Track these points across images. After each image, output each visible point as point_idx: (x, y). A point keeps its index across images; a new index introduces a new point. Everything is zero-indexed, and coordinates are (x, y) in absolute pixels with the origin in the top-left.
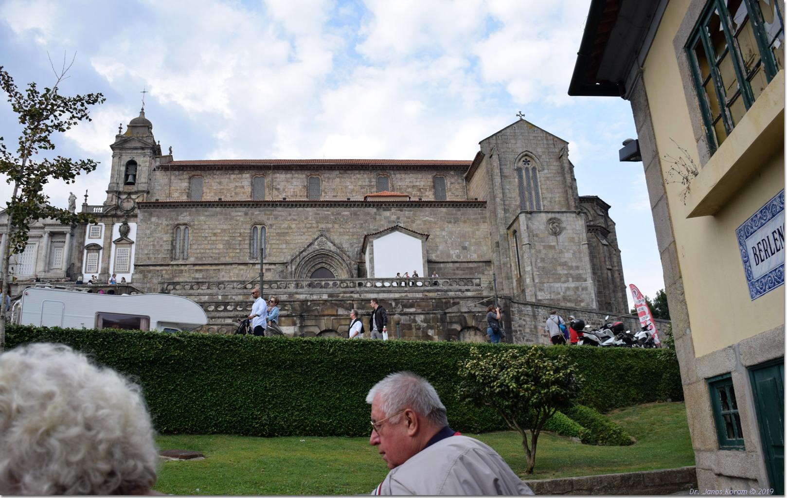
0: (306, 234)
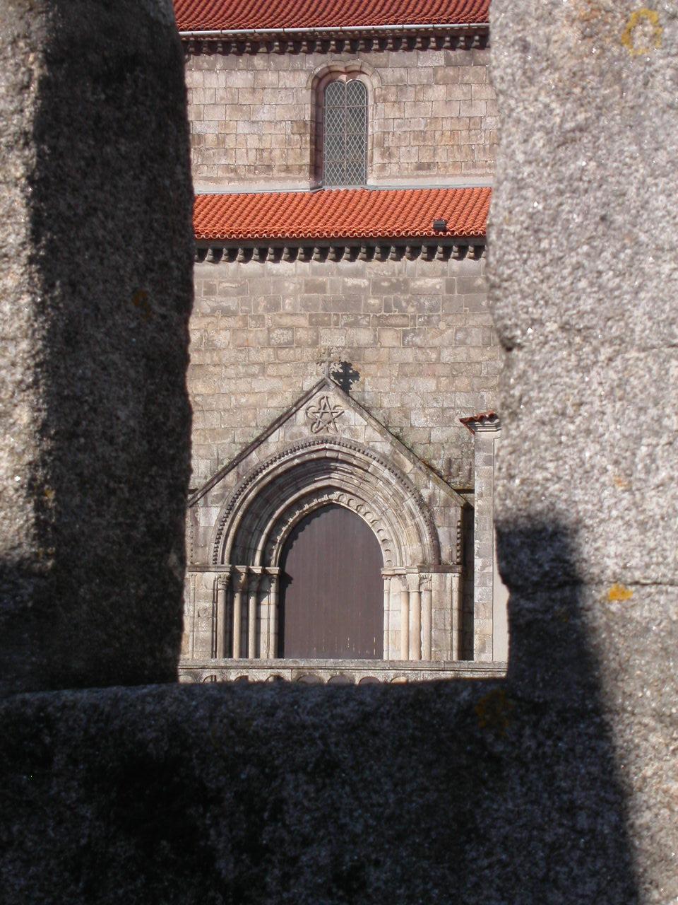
0: (271, 370)
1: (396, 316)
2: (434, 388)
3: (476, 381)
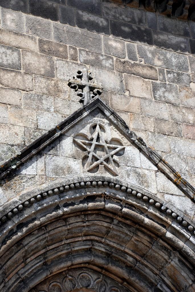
1: (143, 67)
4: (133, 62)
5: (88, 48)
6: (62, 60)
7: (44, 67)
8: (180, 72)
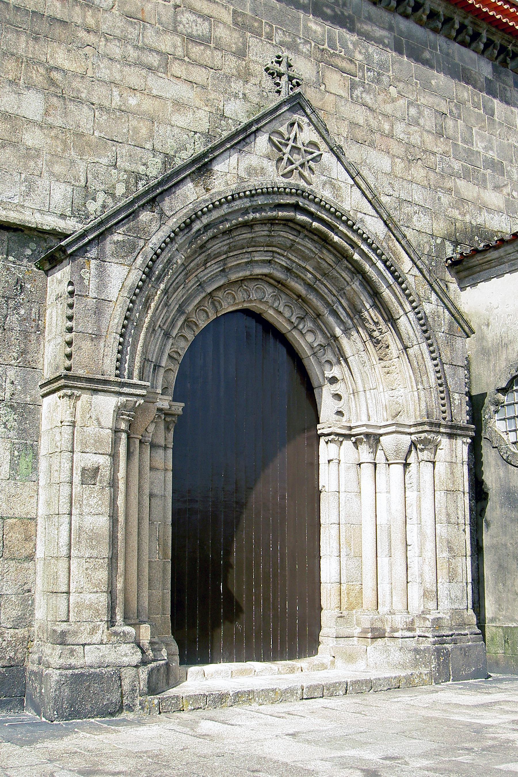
0: (177, 68)
1: (343, 58)
2: (388, 169)
3: (432, 175)
4: (332, 51)
5: (285, 28)
6: (256, 38)
7: (235, 44)
8: (381, 72)
